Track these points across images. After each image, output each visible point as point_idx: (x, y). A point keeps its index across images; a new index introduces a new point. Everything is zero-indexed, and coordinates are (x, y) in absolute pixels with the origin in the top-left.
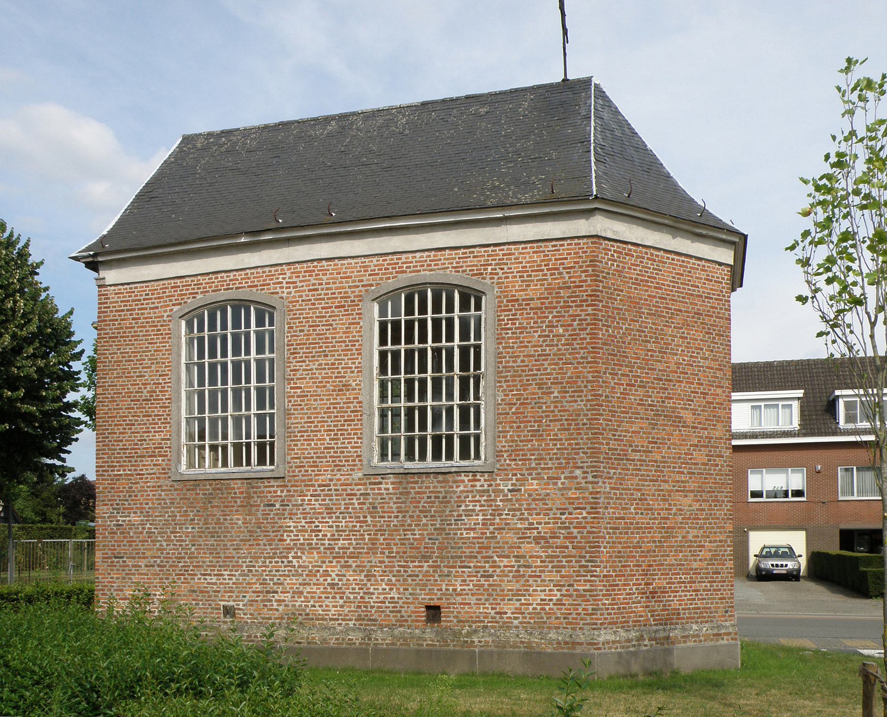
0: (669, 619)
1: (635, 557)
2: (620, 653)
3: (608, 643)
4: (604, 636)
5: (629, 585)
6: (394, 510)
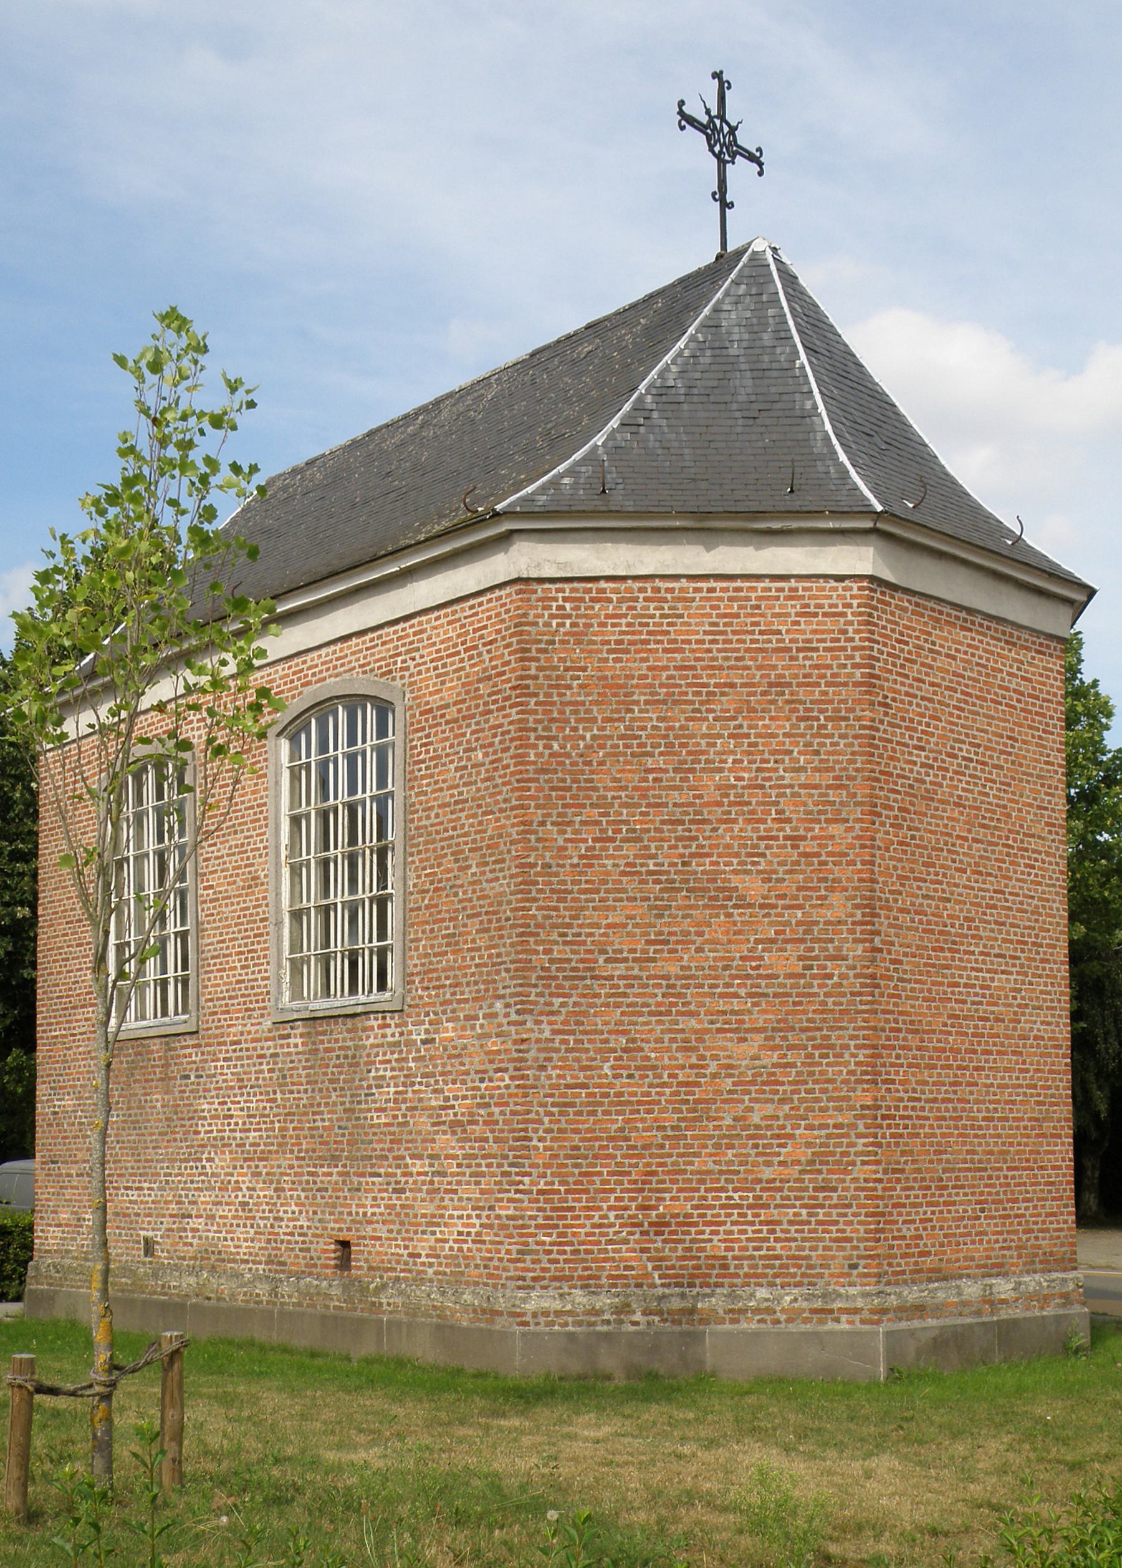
0: (697, 1276)
1: (614, 1157)
2: (571, 1336)
3: (546, 1313)
4: (536, 1300)
5: (600, 1209)
6: (304, 1080)
